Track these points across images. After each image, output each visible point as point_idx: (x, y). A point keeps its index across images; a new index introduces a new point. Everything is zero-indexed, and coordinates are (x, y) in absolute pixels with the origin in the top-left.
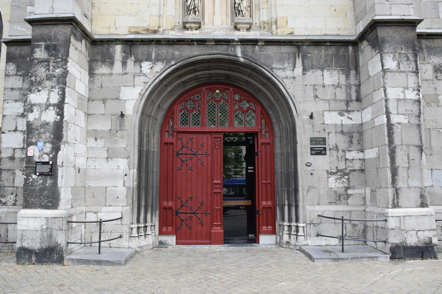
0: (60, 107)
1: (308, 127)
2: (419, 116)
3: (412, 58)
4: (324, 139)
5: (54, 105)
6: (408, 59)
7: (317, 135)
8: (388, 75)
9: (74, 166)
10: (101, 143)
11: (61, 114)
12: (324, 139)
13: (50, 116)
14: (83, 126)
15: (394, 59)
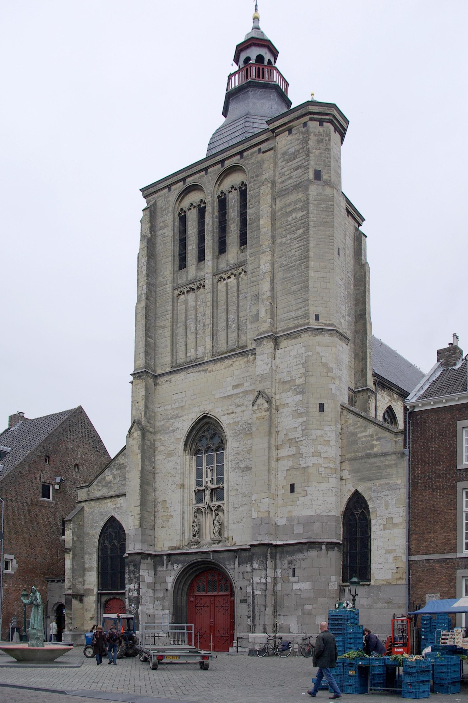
0: (138, 590)
1: (240, 593)
2: (266, 591)
3: (265, 562)
4: (246, 599)
5: (136, 589)
6: (263, 563)
7: (243, 598)
8: (254, 571)
9: (147, 614)
10: (159, 603)
11: (138, 593)
12: (246, 599)
13: (135, 594)
14: (152, 595)
15: (257, 563)
